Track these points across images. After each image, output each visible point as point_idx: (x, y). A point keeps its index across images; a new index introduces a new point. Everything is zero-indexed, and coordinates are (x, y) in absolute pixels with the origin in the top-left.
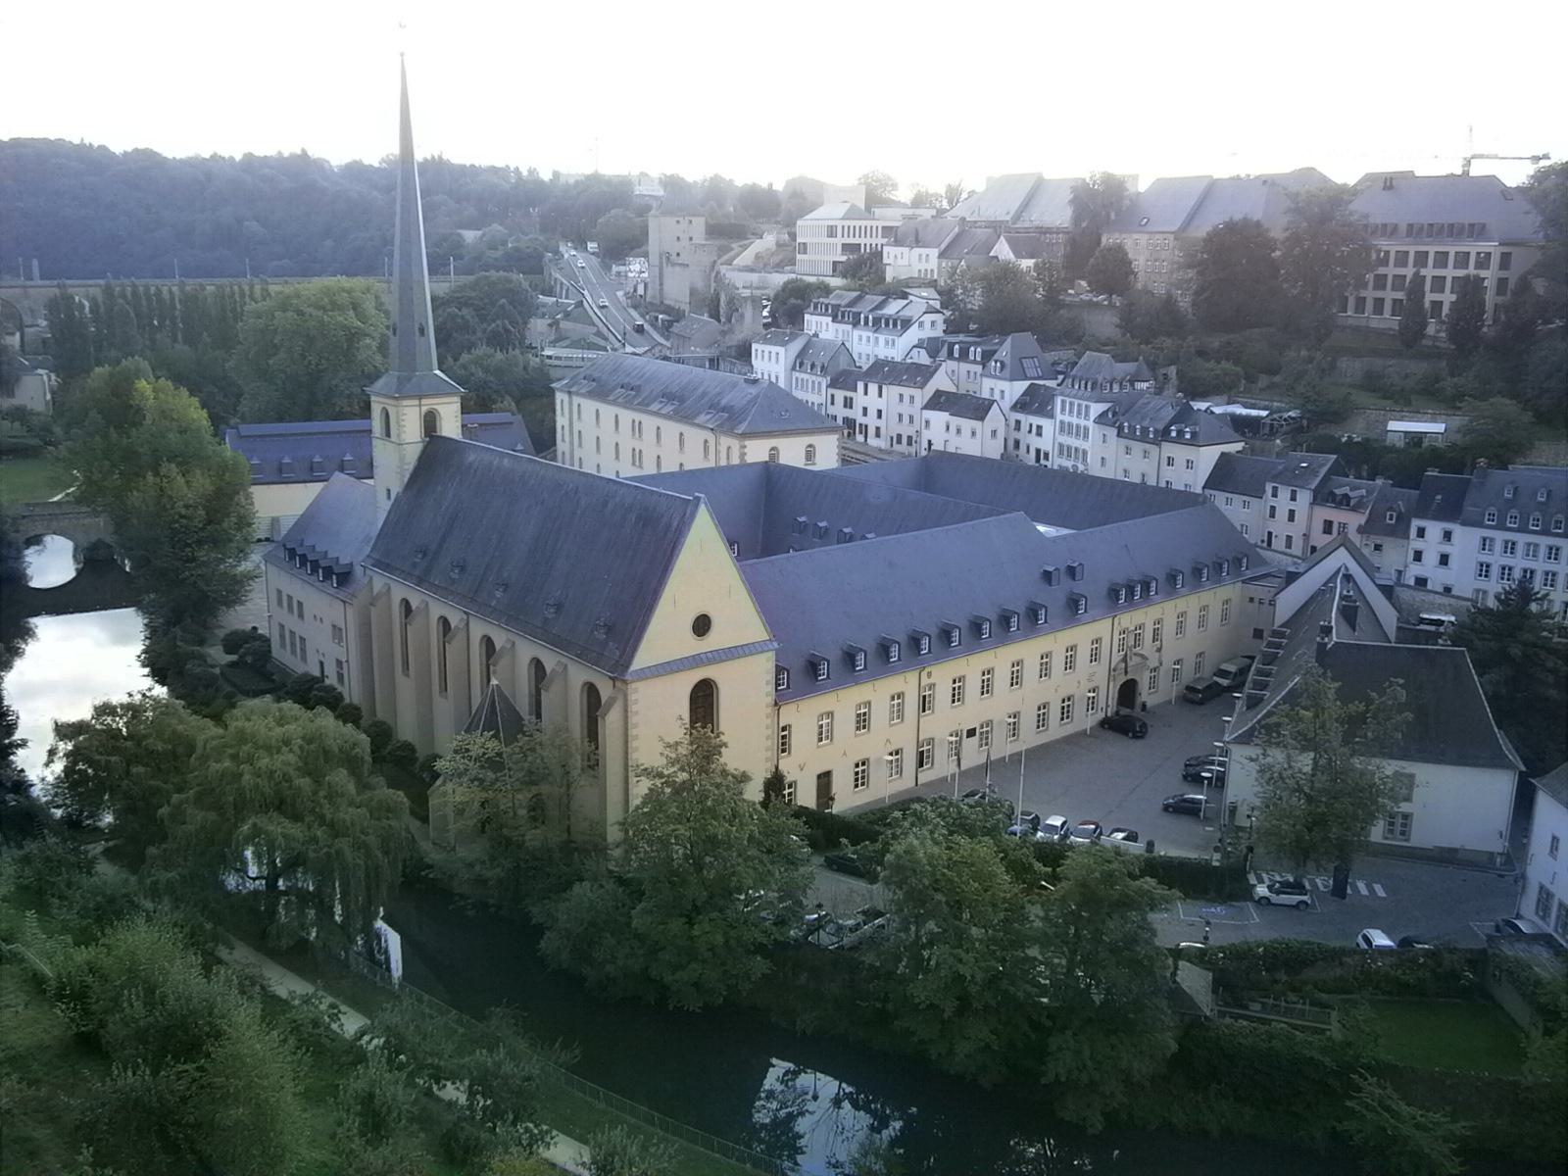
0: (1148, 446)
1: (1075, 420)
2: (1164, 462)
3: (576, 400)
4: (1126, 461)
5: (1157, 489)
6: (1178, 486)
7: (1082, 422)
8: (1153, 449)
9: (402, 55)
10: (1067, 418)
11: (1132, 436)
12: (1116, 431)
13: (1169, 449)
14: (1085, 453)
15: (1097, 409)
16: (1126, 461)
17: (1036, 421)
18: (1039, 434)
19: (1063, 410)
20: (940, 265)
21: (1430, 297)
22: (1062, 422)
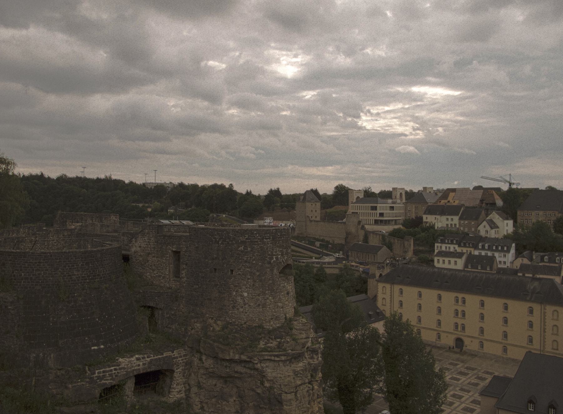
3: (397, 288)
20: (460, 223)
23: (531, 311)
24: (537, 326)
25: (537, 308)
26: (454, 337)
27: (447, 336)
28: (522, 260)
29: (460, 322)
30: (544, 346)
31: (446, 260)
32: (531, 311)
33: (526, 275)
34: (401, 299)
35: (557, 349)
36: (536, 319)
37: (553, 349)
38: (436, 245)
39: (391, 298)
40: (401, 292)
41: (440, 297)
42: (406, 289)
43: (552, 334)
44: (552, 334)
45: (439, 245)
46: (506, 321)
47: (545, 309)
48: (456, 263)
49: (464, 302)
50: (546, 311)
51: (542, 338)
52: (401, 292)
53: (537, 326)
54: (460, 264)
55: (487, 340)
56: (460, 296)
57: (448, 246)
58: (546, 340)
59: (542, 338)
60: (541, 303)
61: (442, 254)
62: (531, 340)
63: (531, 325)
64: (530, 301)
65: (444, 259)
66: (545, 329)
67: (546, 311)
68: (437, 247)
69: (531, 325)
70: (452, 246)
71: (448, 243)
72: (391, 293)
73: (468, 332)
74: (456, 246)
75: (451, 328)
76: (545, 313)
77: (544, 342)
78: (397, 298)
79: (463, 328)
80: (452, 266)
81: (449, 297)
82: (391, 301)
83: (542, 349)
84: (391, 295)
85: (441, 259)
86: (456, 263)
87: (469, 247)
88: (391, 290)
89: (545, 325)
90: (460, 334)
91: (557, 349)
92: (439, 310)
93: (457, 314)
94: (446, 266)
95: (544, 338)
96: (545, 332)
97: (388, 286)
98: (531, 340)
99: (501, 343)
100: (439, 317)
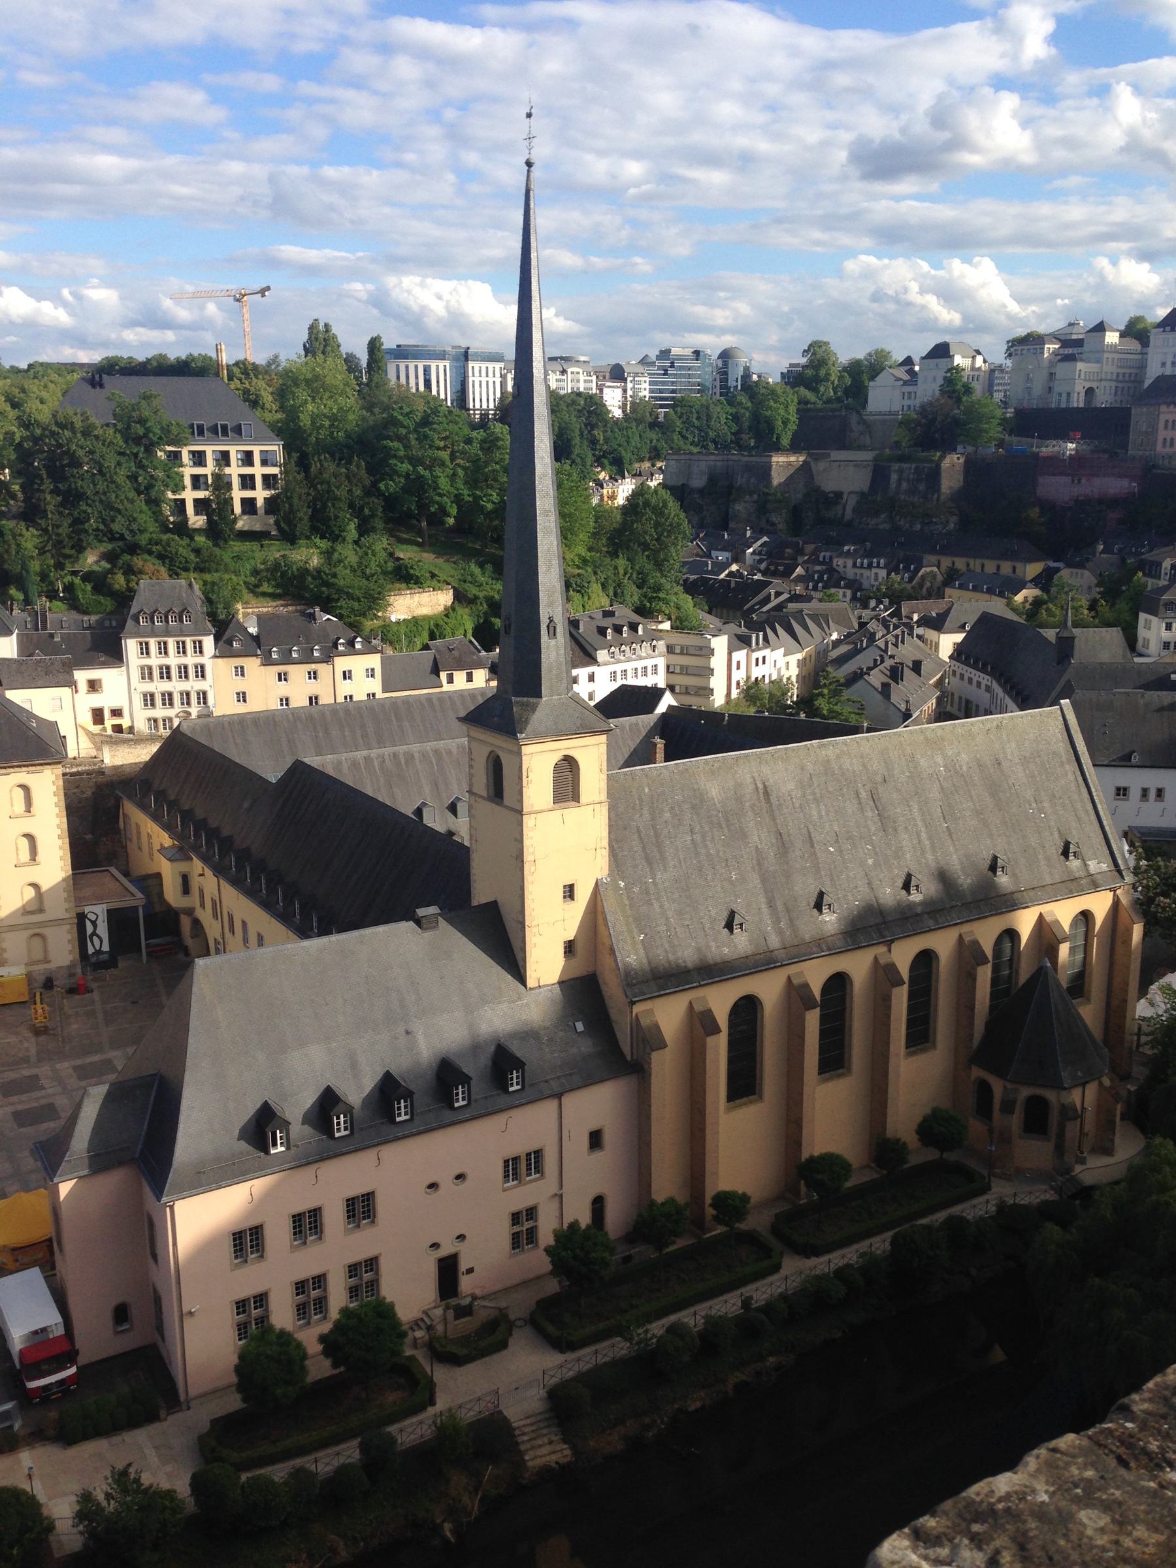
0: (313, 666)
1: (173, 660)
2: (339, 676)
5: (334, 708)
6: (360, 696)
7: (191, 660)
8: (323, 669)
9: (529, 164)
10: (155, 660)
11: (287, 660)
12: (257, 661)
13: (342, 663)
14: (203, 696)
15: (209, 642)
16: (283, 689)
17: (82, 676)
18: (94, 686)
19: (145, 650)
21: (238, 494)
22: (142, 668)
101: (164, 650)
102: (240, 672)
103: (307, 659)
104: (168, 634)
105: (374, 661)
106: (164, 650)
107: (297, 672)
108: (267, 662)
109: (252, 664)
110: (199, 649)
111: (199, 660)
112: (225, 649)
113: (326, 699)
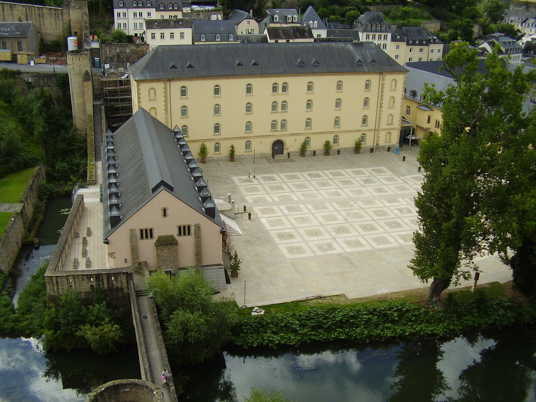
3: (176, 86)
4: (410, 55)
8: (425, 48)
11: (414, 44)
12: (405, 43)
13: (432, 46)
15: (389, 35)
19: (368, 37)
23: (367, 86)
24: (373, 103)
25: (374, 79)
26: (272, 140)
27: (261, 142)
28: (249, 22)
29: (279, 117)
30: (379, 124)
31: (167, 32)
32: (367, 86)
33: (280, 41)
34: (184, 103)
35: (392, 124)
36: (373, 95)
37: (388, 124)
38: (116, 11)
39: (166, 105)
40: (184, 92)
41: (249, 90)
42: (192, 85)
43: (389, 108)
44: (389, 108)
45: (121, 11)
46: (338, 103)
47: (383, 80)
48: (182, 35)
49: (284, 89)
50: (385, 82)
51: (378, 114)
52: (184, 92)
53: (373, 103)
54: (183, 37)
55: (314, 133)
56: (280, 81)
57: (138, 11)
58: (381, 116)
59: (378, 114)
60: (381, 73)
61: (150, 24)
62: (365, 120)
63: (366, 102)
64: (369, 72)
65: (163, 31)
66: (381, 104)
67: (385, 82)
68: (119, 15)
69: (366, 102)
70: (145, 11)
71: (138, 7)
72: (166, 97)
73: (291, 128)
74: (153, 11)
75: (267, 129)
76: (383, 84)
77: (380, 118)
78: (177, 102)
79: (283, 126)
80: (177, 41)
81: (262, 85)
82: (166, 110)
83: (377, 128)
84: (166, 101)
85: (158, 32)
86: (182, 35)
87: (173, 10)
88: (165, 93)
89: (382, 99)
90: (279, 135)
91: (392, 124)
92: (249, 108)
93: (274, 107)
94: (167, 42)
95: (380, 115)
96: (381, 107)
97: (159, 86)
98: (365, 120)
99: (332, 132)
100: (249, 118)
101: (374, 37)
102: (398, 47)
103: (421, 44)
104: (376, 32)
105: (441, 47)
106: (374, 37)
107: (417, 48)
108: (408, 44)
109: (403, 45)
110: (386, 38)
111: (385, 42)
112: (394, 39)
113: (424, 60)
